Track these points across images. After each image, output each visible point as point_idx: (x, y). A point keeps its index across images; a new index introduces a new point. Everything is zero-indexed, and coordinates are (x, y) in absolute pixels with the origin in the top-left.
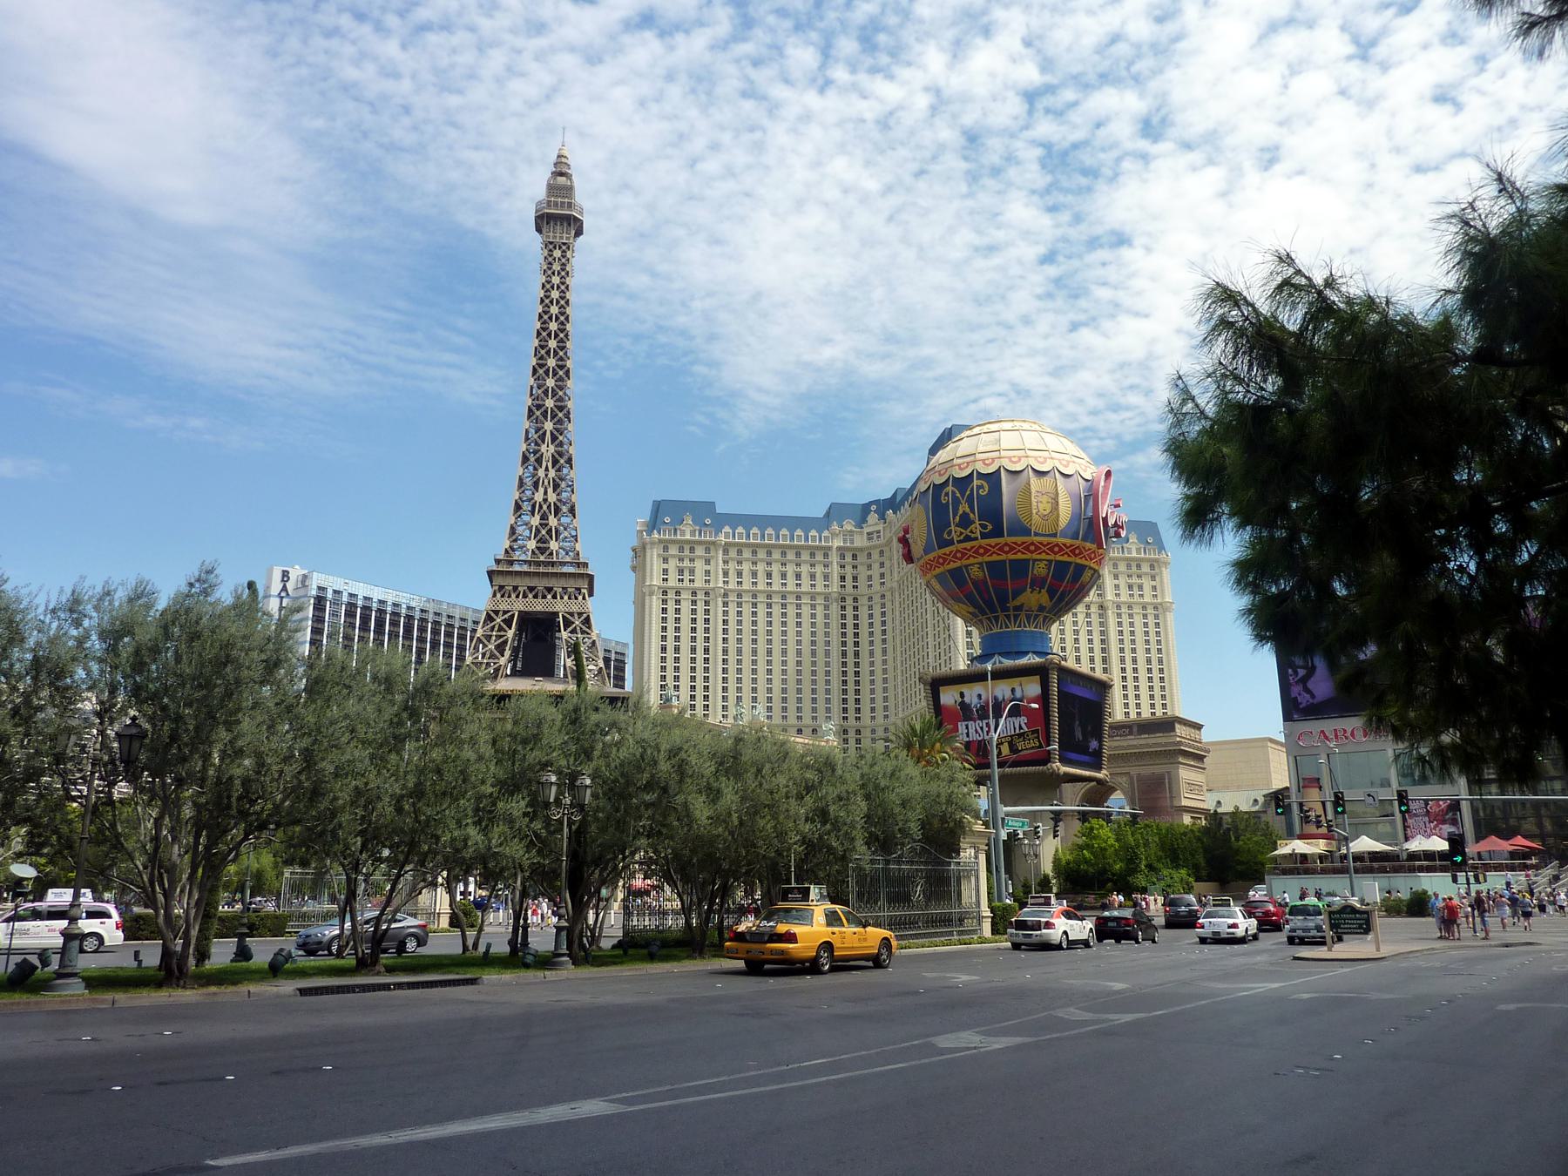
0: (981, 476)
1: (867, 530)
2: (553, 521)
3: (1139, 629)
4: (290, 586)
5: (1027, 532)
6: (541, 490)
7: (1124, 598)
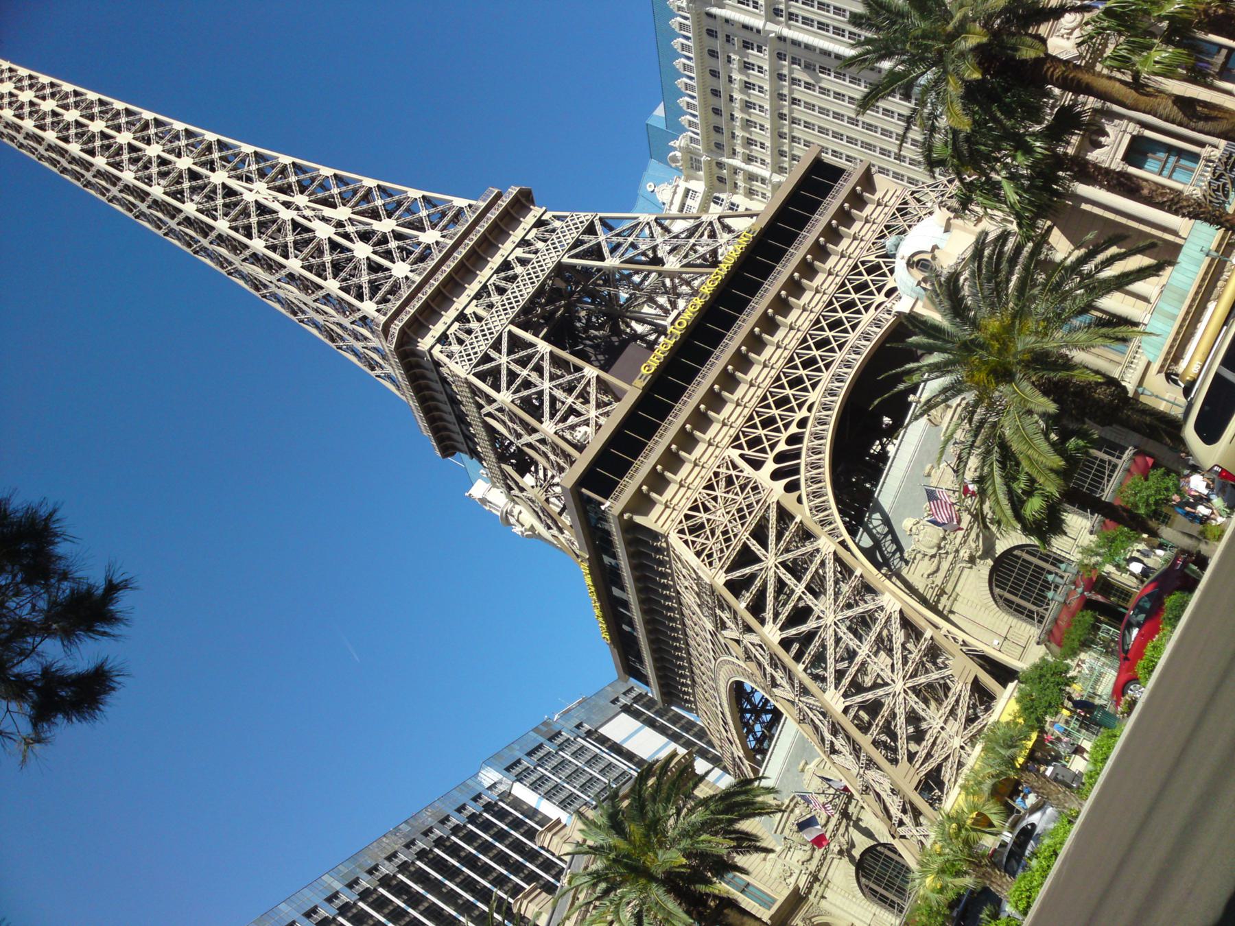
6: (317, 225)
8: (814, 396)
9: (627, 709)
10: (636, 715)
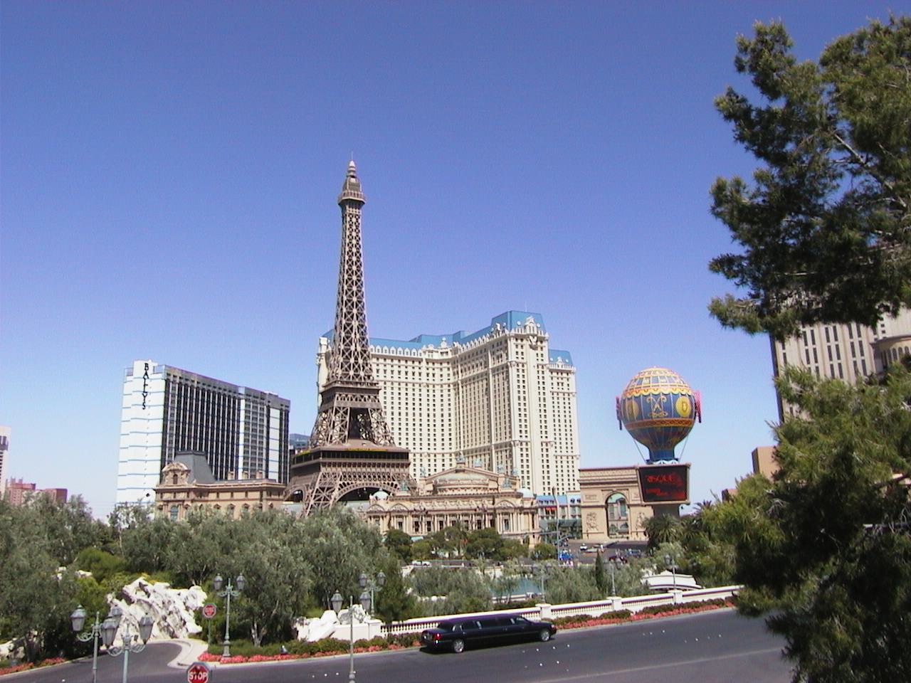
0: (664, 394)
1: (440, 351)
2: (360, 361)
3: (561, 405)
4: (149, 372)
5: (679, 416)
6: (354, 344)
7: (555, 389)
8: (358, 482)
9: (281, 410)
10: (281, 414)
